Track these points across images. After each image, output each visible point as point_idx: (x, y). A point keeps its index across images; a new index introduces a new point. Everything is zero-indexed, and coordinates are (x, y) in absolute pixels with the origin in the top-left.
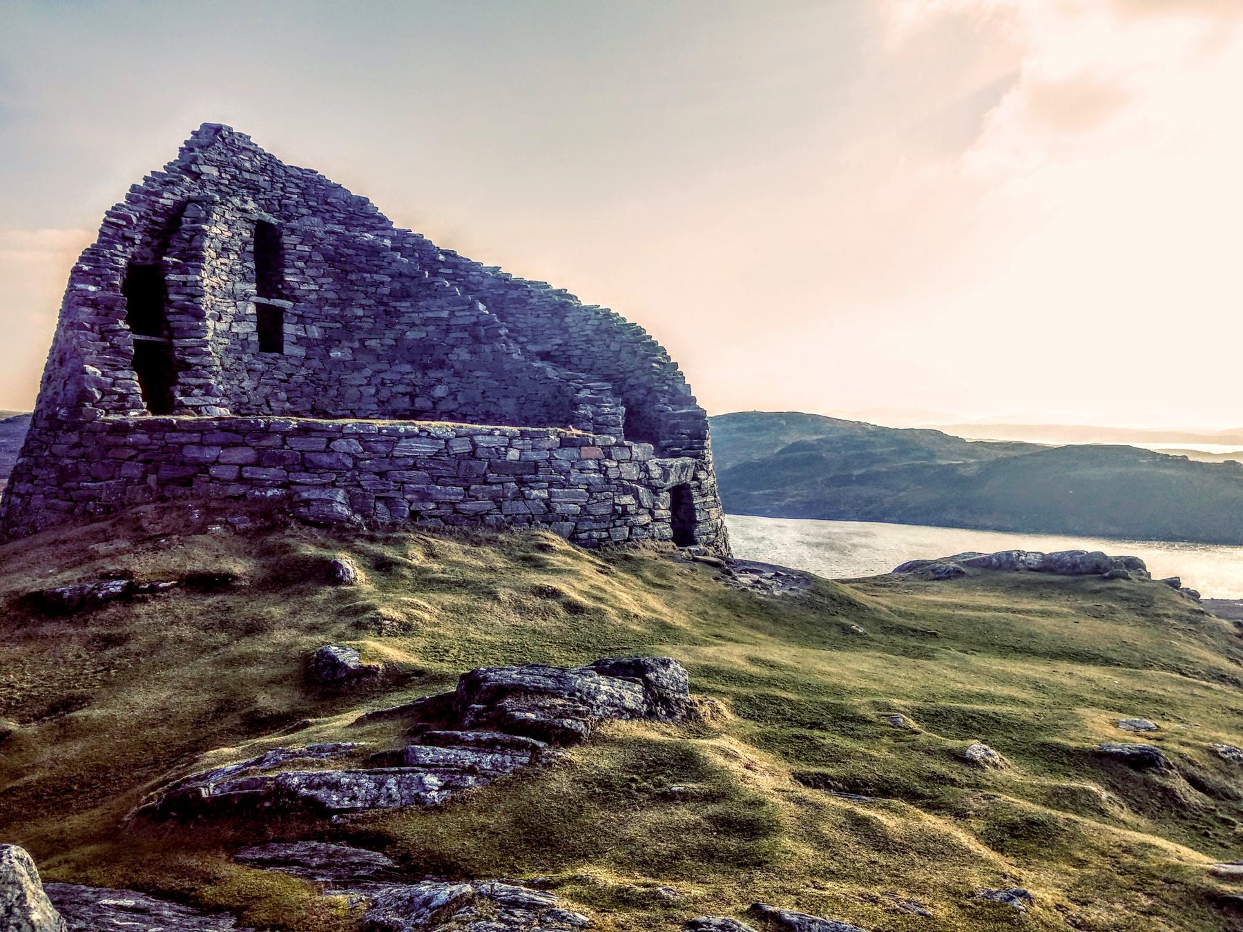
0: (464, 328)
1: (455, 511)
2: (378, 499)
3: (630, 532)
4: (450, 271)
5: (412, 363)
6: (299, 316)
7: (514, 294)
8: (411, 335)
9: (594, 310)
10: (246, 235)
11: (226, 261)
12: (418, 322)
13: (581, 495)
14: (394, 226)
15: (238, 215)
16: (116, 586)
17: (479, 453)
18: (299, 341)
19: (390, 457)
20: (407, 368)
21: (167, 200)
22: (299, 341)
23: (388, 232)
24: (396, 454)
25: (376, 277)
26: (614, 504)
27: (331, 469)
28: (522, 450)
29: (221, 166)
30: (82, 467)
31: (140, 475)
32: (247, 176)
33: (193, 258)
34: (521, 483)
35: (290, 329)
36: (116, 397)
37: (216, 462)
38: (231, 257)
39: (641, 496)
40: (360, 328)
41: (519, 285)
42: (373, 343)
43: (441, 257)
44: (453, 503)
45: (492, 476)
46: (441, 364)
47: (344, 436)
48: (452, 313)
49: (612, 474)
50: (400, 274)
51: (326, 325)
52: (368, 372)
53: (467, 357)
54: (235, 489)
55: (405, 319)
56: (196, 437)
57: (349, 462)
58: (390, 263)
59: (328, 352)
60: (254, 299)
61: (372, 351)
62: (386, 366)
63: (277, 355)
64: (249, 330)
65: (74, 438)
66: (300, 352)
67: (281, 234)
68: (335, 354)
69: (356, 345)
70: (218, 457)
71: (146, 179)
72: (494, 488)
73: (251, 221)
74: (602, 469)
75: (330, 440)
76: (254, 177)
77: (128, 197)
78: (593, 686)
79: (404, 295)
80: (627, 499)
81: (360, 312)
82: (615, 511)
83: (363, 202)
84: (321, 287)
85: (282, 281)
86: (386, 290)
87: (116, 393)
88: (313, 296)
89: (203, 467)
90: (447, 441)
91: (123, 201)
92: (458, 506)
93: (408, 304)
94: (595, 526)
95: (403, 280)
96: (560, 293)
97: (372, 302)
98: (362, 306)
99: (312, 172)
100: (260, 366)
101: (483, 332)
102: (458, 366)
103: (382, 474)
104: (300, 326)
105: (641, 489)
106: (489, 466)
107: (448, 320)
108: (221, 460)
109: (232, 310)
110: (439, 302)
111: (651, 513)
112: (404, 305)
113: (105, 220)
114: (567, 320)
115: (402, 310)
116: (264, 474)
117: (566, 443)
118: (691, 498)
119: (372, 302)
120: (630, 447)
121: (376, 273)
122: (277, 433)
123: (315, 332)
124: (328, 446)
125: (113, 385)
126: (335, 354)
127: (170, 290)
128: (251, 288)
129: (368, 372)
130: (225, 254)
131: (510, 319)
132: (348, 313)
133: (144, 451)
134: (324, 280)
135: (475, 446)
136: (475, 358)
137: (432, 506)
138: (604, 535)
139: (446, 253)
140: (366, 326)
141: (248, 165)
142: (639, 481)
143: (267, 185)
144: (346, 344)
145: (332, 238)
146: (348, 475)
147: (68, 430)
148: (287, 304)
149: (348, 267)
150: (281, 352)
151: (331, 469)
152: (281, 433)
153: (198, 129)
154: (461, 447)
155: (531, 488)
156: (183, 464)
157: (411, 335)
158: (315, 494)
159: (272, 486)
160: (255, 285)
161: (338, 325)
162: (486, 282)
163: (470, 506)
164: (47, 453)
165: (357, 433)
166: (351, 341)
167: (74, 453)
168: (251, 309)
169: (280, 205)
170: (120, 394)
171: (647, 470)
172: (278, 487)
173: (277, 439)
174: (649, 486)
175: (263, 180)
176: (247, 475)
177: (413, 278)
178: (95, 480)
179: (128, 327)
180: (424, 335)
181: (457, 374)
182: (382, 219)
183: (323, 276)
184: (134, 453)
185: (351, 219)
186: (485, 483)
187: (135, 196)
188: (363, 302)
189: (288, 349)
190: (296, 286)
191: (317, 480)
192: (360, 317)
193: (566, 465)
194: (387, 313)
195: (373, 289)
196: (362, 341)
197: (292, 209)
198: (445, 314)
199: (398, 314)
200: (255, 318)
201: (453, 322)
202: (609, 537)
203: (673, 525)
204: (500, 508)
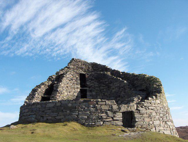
2: (41, 117)
3: (103, 123)
7: (136, 78)
8: (113, 91)
11: (72, 82)
14: (112, 69)
15: (75, 73)
19: (45, 107)
28: (72, 104)
29: (74, 65)
35: (88, 93)
38: (73, 81)
39: (108, 113)
41: (137, 75)
43: (121, 73)
48: (120, 84)
55: (111, 88)
73: (79, 74)
75: (37, 105)
76: (82, 66)
79: (111, 82)
80: (102, 115)
82: (99, 118)
83: (104, 66)
88: (93, 86)
95: (110, 79)
98: (103, 87)
99: (94, 63)
102: (122, 96)
109: (74, 91)
110: (117, 83)
111: (112, 118)
112: (111, 85)
118: (134, 115)
120: (105, 101)
121: (105, 79)
128: (79, 86)
134: (95, 83)
137: (51, 117)
138: (93, 123)
139: (123, 73)
142: (109, 110)
148: (87, 88)
149: (100, 79)
155: (74, 112)
157: (113, 91)
163: (58, 118)
169: (88, 70)
171: (112, 107)
175: (83, 66)
177: (112, 79)
183: (95, 82)
186: (63, 112)
187: (57, 73)
195: (105, 83)
196: (104, 94)
198: (119, 85)
202: (95, 124)
203: (123, 122)
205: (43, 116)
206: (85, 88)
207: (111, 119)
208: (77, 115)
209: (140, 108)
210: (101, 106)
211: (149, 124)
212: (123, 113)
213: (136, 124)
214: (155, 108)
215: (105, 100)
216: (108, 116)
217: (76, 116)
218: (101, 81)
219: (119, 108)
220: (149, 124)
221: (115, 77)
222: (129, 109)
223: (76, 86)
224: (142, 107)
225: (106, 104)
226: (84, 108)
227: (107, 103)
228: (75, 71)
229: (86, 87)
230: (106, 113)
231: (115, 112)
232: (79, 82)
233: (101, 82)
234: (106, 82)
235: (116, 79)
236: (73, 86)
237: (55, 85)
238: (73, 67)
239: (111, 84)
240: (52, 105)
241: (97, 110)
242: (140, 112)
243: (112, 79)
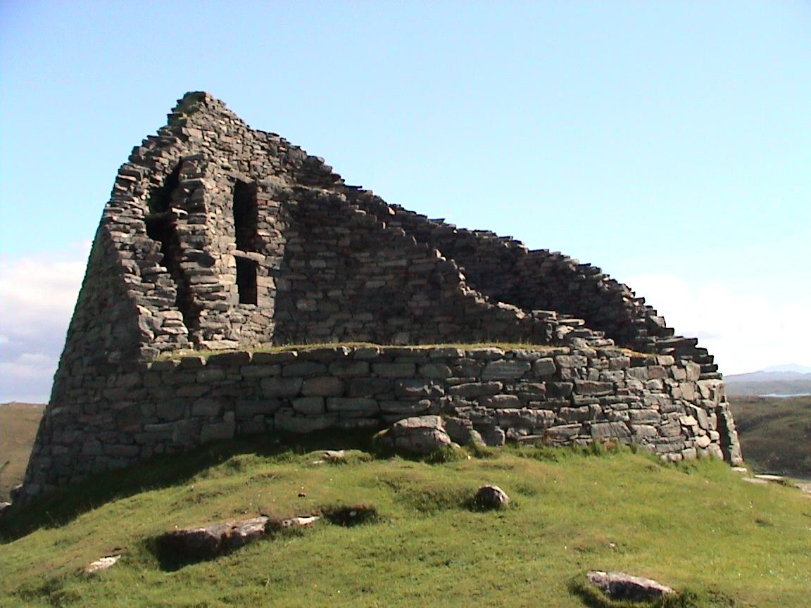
0: (421, 276)
5: (373, 312)
7: (460, 243)
8: (369, 284)
9: (541, 255)
10: (228, 190)
12: (377, 271)
13: (655, 417)
14: (346, 183)
15: (223, 172)
16: (256, 524)
20: (369, 316)
25: (339, 230)
26: (682, 425)
30: (146, 409)
31: (216, 413)
32: (223, 138)
33: (196, 209)
36: (167, 337)
40: (324, 280)
42: (334, 293)
45: (578, 398)
46: (400, 313)
47: (432, 361)
48: (410, 263)
49: (675, 392)
50: (359, 226)
51: (292, 277)
52: (331, 322)
53: (427, 303)
54: (320, 423)
55: (364, 270)
56: (275, 370)
58: (349, 217)
60: (235, 252)
61: (335, 301)
62: (346, 316)
63: (253, 306)
64: (231, 283)
65: (133, 379)
67: (256, 192)
68: (301, 305)
69: (320, 295)
70: (301, 389)
74: (667, 389)
76: (228, 140)
79: (363, 245)
81: (323, 264)
82: (682, 432)
86: (347, 242)
87: (166, 333)
89: (285, 401)
91: (127, 161)
93: (368, 254)
97: (333, 254)
98: (325, 259)
100: (240, 317)
101: (442, 278)
105: (699, 409)
107: (407, 269)
108: (305, 392)
112: (364, 256)
113: (117, 178)
114: (518, 264)
115: (363, 260)
119: (333, 254)
122: (362, 360)
124: (417, 372)
126: (301, 305)
129: (331, 322)
132: (315, 264)
133: (218, 387)
135: (559, 368)
136: (434, 303)
139: (393, 207)
140: (328, 277)
142: (694, 402)
143: (239, 147)
144: (310, 295)
147: (124, 373)
150: (256, 305)
152: (367, 360)
153: (181, 97)
156: (262, 398)
158: (416, 422)
160: (234, 239)
164: (97, 398)
166: (315, 292)
167: (135, 394)
168: (233, 263)
169: (249, 166)
170: (171, 334)
171: (699, 390)
172: (370, 418)
173: (363, 368)
174: (702, 406)
175: (235, 144)
177: (371, 229)
178: (161, 421)
179: (164, 269)
180: (384, 283)
181: (416, 320)
184: (206, 389)
185: (309, 177)
186: (573, 405)
188: (328, 254)
189: (260, 302)
190: (267, 239)
193: (639, 386)
195: (335, 242)
196: (325, 292)
197: (260, 170)
198: (403, 262)
199: (359, 264)
200: (235, 271)
201: (411, 269)
210: (678, 386)
218: (317, 230)
232: (232, 221)
234: (339, 237)
239: (360, 250)
243: (371, 229)
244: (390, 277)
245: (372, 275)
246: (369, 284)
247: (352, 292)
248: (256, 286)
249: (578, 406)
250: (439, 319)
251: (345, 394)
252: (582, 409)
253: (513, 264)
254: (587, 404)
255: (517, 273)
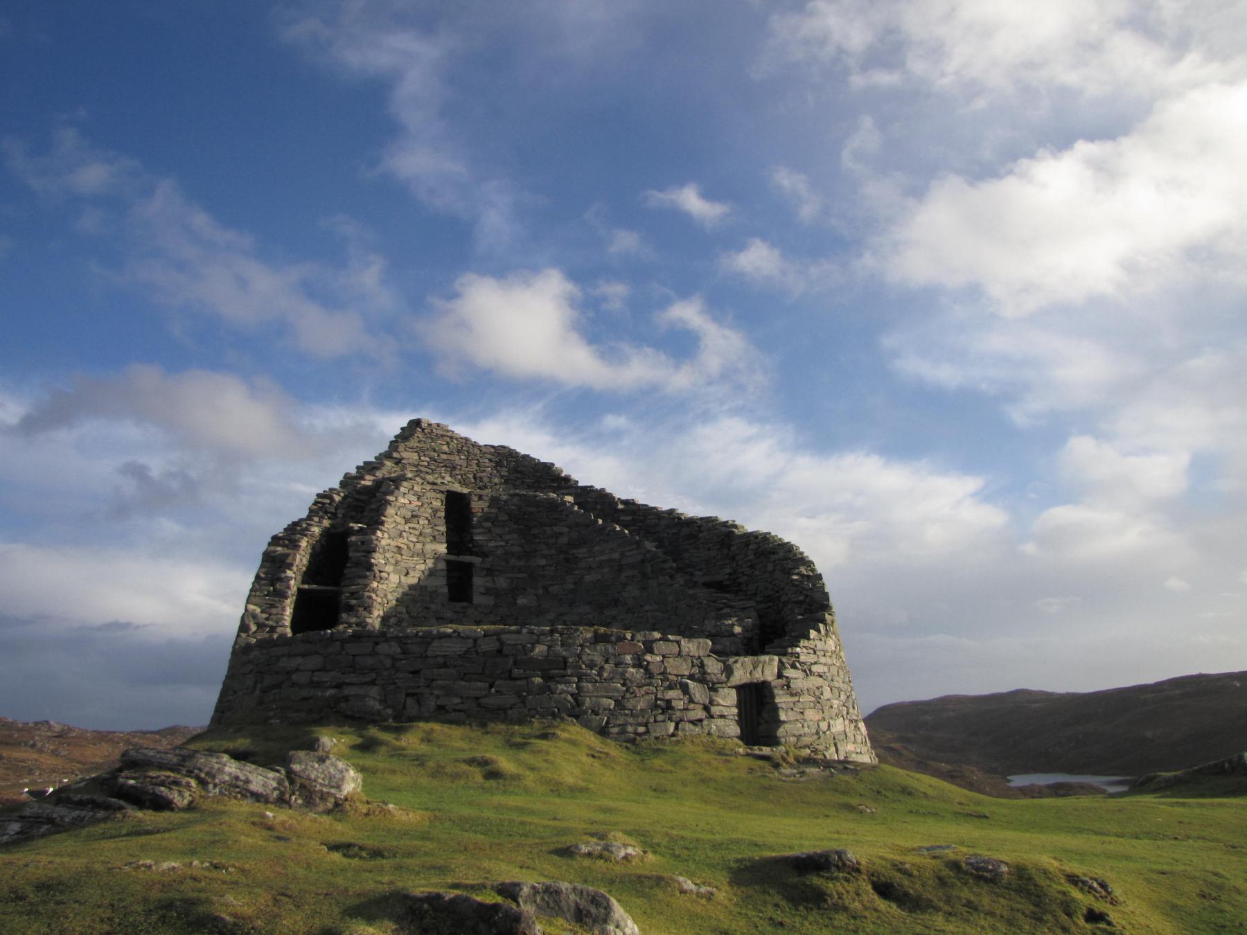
1: (479, 705)
2: (407, 695)
3: (676, 728)
4: (629, 518)
6: (488, 570)
7: (686, 531)
8: (588, 578)
10: (437, 504)
11: (417, 526)
15: (429, 487)
17: (506, 650)
18: (488, 592)
21: (368, 481)
22: (488, 592)
23: (573, 491)
24: (429, 653)
25: (555, 529)
27: (373, 670)
29: (420, 451)
32: (444, 456)
33: (376, 522)
34: (548, 678)
35: (478, 582)
37: (297, 670)
39: (692, 691)
41: (691, 522)
42: (554, 589)
43: (620, 506)
44: (477, 698)
47: (387, 640)
54: (305, 693)
57: (388, 662)
59: (515, 599)
63: (466, 604)
66: (488, 601)
68: (521, 601)
69: (540, 591)
71: (358, 468)
72: (519, 683)
75: (377, 644)
76: (451, 457)
77: (341, 483)
78: (216, 766)
80: (671, 694)
81: (543, 562)
82: (657, 706)
83: (548, 467)
84: (507, 542)
85: (472, 540)
86: (564, 540)
87: (267, 626)
90: (475, 640)
92: (481, 701)
94: (631, 720)
96: (725, 524)
98: (545, 557)
103: (415, 672)
104: (489, 578)
106: (515, 663)
112: (581, 552)
116: (326, 677)
117: (598, 638)
118: (773, 696)
119: (553, 552)
120: (678, 642)
121: (556, 525)
123: (502, 582)
125: (267, 619)
127: (351, 549)
130: (415, 520)
131: (686, 555)
134: (508, 537)
135: (502, 643)
137: (457, 700)
138: (641, 729)
139: (626, 502)
141: (445, 448)
142: (691, 677)
145: (516, 500)
146: (386, 673)
148: (476, 560)
151: (373, 670)
154: (488, 646)
159: (330, 687)
161: (524, 575)
162: (663, 523)
163: (492, 701)
165: (397, 637)
169: (475, 478)
171: (702, 666)
175: (459, 460)
176: (315, 679)
182: (567, 479)
183: (509, 533)
186: (511, 678)
187: (347, 481)
188: (546, 552)
189: (477, 599)
191: (363, 680)
192: (543, 567)
193: (599, 659)
194: (567, 560)
195: (553, 541)
196: (545, 588)
197: (486, 480)
198: (616, 556)
200: (445, 573)
202: (648, 732)
203: (739, 723)
204: (523, 702)
205: (418, 691)
206: (467, 559)
207: (701, 714)
208: (572, 695)
209: (789, 673)
211: (817, 733)
212: (741, 689)
213: (781, 730)
214: (826, 669)
215: (678, 638)
216: (691, 701)
217: (569, 698)
218: (535, 531)
219: (728, 671)
220: (817, 733)
221: (600, 521)
222: (758, 676)
223: (430, 547)
224: (793, 666)
225: (680, 654)
226: (602, 668)
227: (685, 651)
228: (430, 478)
229: (472, 553)
230: (685, 689)
231: (713, 688)
232: (443, 529)
233: (535, 536)
234: (558, 535)
235: (603, 528)
236: (419, 546)
237: (353, 538)
238: (415, 456)
240: (456, 648)
241: (649, 675)
242: (789, 687)
244: (606, 570)
245: (590, 568)
246: (588, 578)
247: (572, 586)
248: (471, 586)
249: (516, 679)
250: (647, 607)
251: (323, 669)
252: (523, 683)
253: (729, 547)
254: (526, 678)
255: (733, 558)
